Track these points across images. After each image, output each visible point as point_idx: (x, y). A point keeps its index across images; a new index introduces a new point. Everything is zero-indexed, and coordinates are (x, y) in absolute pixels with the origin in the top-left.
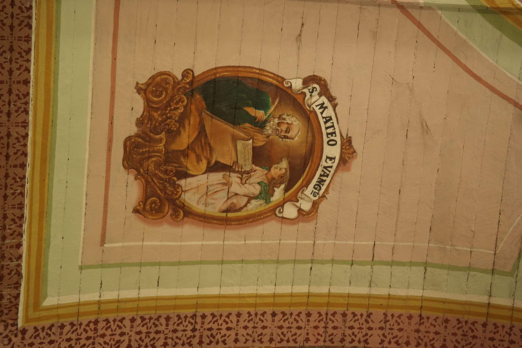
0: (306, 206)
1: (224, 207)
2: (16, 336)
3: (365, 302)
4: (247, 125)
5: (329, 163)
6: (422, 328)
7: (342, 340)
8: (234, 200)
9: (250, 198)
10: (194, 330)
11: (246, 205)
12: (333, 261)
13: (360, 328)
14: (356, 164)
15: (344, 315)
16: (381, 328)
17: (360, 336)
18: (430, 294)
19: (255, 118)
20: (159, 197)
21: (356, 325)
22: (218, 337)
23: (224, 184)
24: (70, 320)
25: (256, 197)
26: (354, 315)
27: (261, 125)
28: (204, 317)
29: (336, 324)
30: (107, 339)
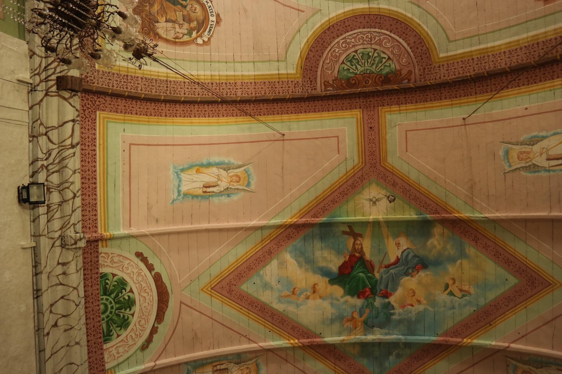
0: (206, 39)
1: (174, 37)
2: (95, 72)
3: (233, 78)
4: (179, 6)
5: (212, 23)
6: (256, 87)
7: (227, 94)
8: (178, 34)
9: (184, 35)
10: (167, 87)
11: (182, 37)
12: (219, 62)
13: (233, 89)
14: (222, 23)
15: (226, 84)
16: (241, 88)
17: (233, 92)
18: (257, 73)
19: (182, 4)
20: (148, 28)
21: (231, 88)
22: (177, 91)
23: (173, 28)
24: (117, 72)
25: (186, 35)
26: (230, 83)
27: (185, 7)
28: (170, 82)
29: (223, 87)
30: (132, 84)
